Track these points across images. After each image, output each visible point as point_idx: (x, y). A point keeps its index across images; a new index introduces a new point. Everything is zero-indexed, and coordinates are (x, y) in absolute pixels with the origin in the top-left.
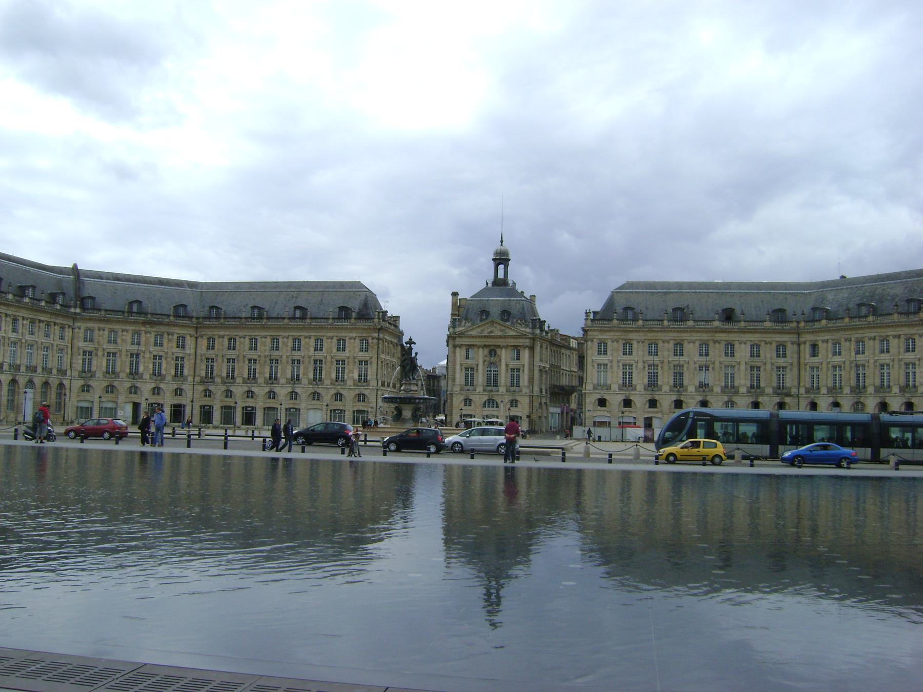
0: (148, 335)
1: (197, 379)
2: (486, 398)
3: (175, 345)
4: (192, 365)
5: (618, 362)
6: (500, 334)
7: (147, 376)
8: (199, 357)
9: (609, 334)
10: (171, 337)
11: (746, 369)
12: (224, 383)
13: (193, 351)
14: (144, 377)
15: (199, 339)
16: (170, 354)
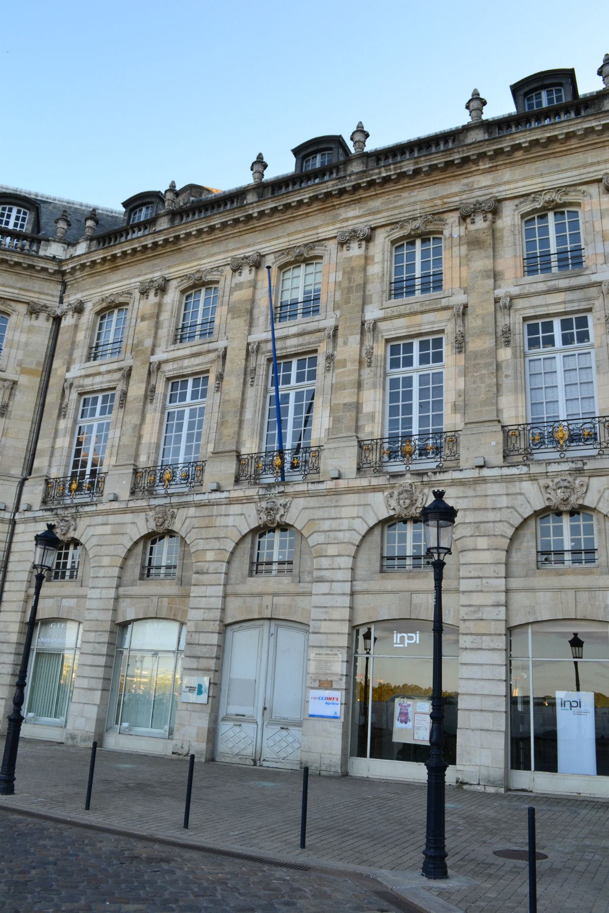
0: (356, 250)
3: (510, 259)
7: (341, 459)
10: (480, 223)
14: (329, 463)
16: (482, 309)
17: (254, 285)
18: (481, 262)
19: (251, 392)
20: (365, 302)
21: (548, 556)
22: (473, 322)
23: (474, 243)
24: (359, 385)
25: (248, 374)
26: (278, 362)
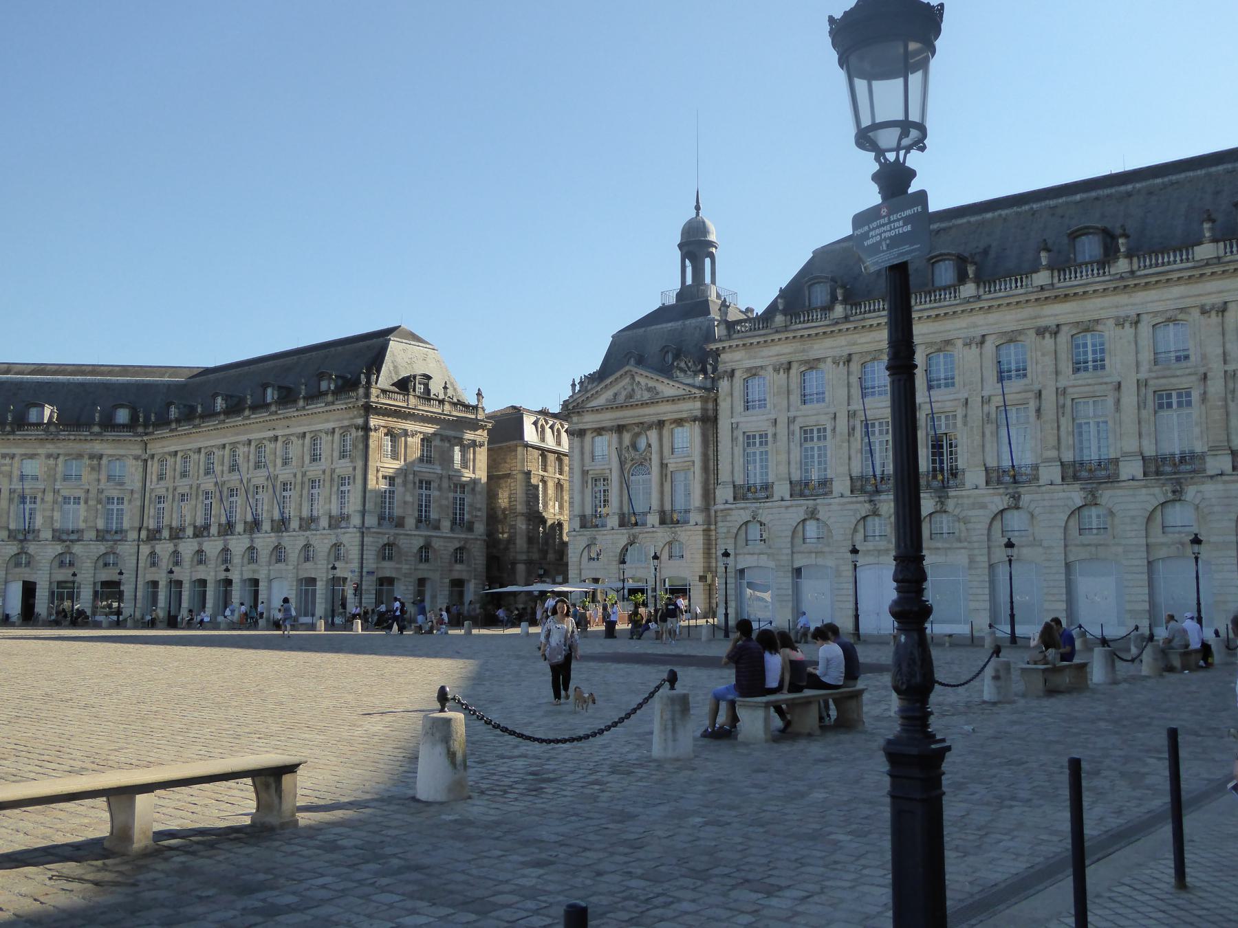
0: (52, 461)
1: (144, 534)
2: (623, 541)
3: (103, 477)
4: (137, 512)
5: (791, 421)
6: (646, 396)
7: (46, 534)
8: (147, 495)
9: (766, 352)
10: (95, 462)
11: (1141, 405)
12: (171, 538)
13: (138, 485)
14: (43, 535)
15: (149, 463)
16: (93, 492)
17: (11, 465)
18: (94, 476)
19: (12, 508)
20: (55, 480)
21: (106, 565)
22: (91, 495)
23: (93, 469)
24: (53, 510)
25: (11, 500)
26: (23, 499)
